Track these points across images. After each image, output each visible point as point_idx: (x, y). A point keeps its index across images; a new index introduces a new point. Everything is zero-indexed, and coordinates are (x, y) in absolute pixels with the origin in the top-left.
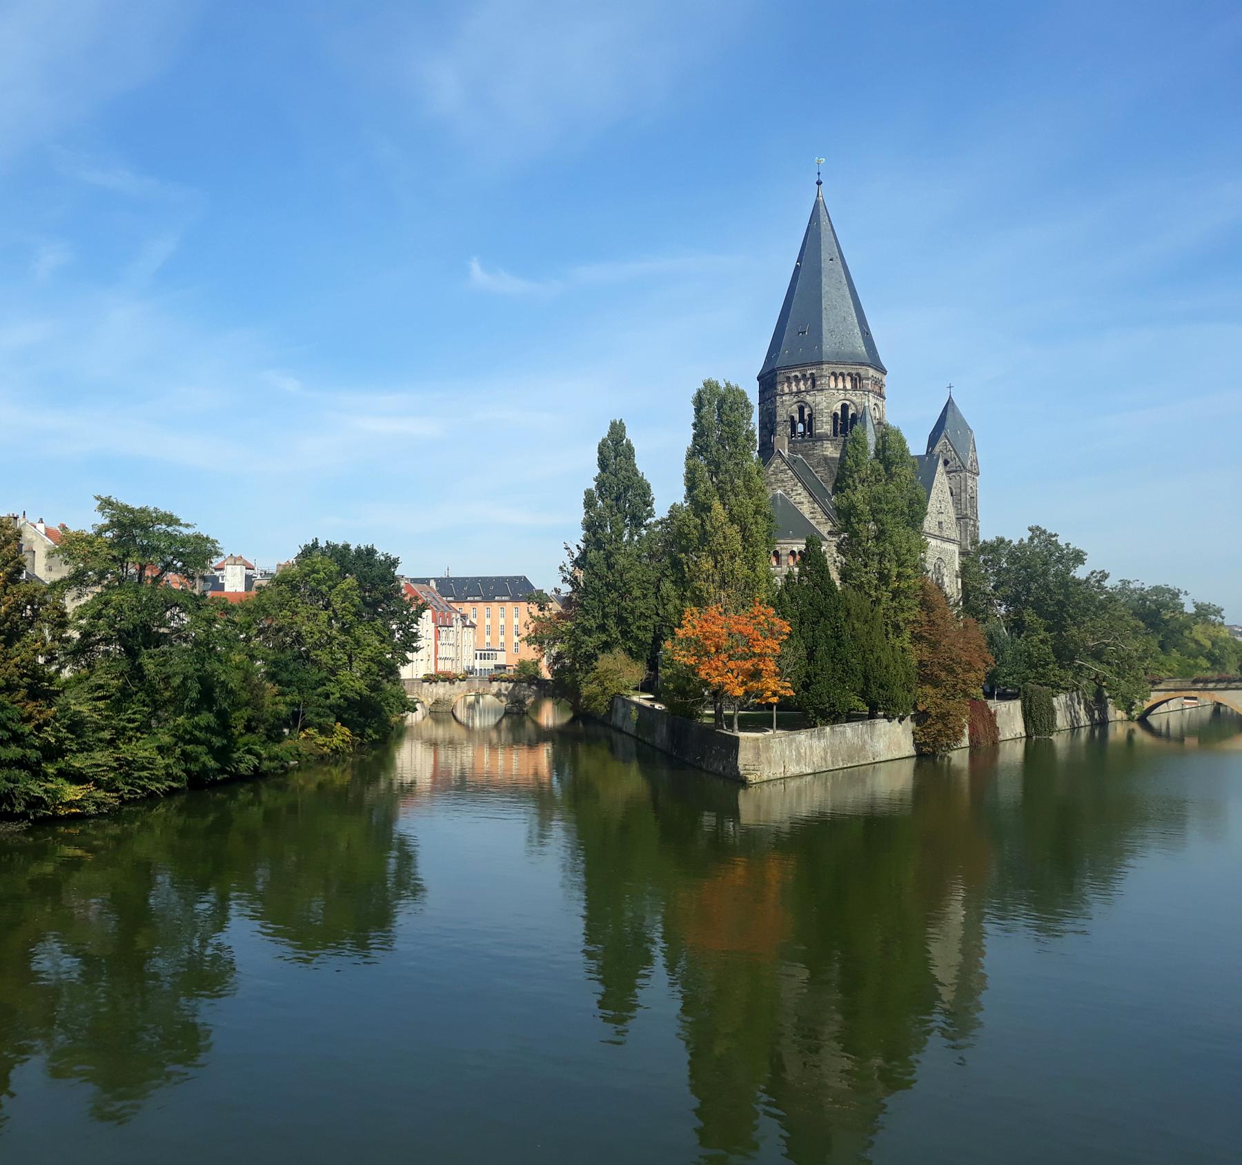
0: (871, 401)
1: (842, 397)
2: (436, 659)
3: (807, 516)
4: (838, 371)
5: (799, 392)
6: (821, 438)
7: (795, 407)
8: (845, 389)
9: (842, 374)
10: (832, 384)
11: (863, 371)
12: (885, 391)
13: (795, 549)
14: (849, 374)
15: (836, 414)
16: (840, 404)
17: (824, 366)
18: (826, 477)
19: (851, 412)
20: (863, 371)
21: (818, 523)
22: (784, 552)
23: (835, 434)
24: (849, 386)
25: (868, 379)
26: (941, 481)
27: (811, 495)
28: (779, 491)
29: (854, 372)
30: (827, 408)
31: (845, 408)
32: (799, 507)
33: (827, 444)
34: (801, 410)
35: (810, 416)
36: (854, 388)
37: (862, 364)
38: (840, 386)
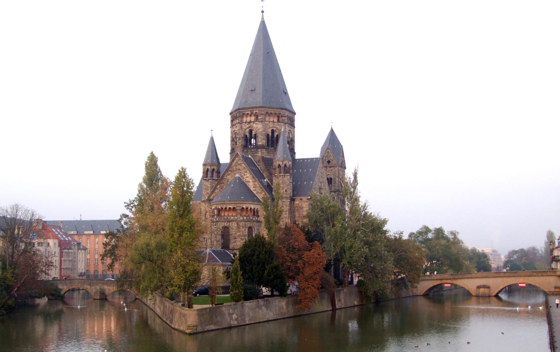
0: (288, 128)
1: (271, 126)
2: (61, 269)
3: (252, 189)
4: (270, 112)
5: (250, 122)
6: (262, 147)
7: (248, 130)
8: (273, 122)
9: (271, 113)
10: (267, 119)
11: (282, 112)
12: (296, 123)
13: (244, 207)
14: (275, 114)
15: (268, 135)
16: (270, 130)
18: (263, 169)
19: (276, 134)
20: (282, 112)
21: (257, 193)
22: (238, 208)
23: (268, 145)
24: (276, 120)
25: (285, 117)
27: (253, 178)
28: (237, 175)
29: (278, 113)
30: (263, 131)
31: (273, 131)
32: (248, 184)
33: (264, 151)
34: (251, 131)
35: (255, 135)
36: (278, 121)
37: (282, 109)
38: (271, 119)
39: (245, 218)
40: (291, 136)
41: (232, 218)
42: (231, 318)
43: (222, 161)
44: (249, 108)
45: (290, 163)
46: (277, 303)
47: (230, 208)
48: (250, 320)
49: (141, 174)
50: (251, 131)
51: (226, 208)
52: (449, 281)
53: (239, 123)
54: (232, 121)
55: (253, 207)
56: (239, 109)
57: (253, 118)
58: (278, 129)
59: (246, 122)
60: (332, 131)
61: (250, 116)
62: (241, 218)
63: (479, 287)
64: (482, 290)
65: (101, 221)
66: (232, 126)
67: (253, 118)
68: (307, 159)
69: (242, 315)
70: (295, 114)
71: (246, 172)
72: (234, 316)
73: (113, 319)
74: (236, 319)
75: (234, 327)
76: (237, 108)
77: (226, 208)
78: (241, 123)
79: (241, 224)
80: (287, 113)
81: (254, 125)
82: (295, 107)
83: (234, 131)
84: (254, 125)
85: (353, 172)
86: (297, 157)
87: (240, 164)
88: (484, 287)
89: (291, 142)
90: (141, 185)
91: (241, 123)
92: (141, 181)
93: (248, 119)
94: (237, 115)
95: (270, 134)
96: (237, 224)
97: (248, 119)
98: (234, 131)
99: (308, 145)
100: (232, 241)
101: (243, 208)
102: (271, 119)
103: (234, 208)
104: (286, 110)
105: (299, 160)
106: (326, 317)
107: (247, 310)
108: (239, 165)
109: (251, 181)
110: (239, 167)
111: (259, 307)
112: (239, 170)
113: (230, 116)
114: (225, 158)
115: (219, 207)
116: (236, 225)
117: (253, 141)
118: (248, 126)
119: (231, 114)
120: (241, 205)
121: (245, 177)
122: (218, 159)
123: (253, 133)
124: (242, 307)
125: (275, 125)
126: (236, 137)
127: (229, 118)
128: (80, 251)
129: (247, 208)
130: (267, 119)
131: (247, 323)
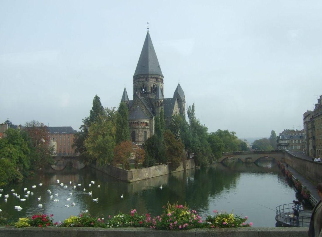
1: (153, 83)
5: (143, 81)
7: (142, 85)
9: (153, 77)
13: (142, 122)
14: (155, 77)
15: (152, 87)
16: (152, 85)
17: (149, 75)
19: (155, 87)
23: (152, 92)
24: (155, 80)
26: (176, 104)
29: (156, 77)
31: (154, 86)
33: (150, 95)
34: (143, 86)
35: (146, 87)
36: (157, 81)
39: (142, 127)
40: (162, 88)
41: (136, 127)
42: (146, 175)
43: (130, 100)
44: (143, 75)
45: (163, 101)
46: (163, 167)
47: (135, 122)
48: (153, 176)
49: (90, 106)
50: (143, 86)
51: (133, 122)
52: (233, 156)
53: (138, 82)
54: (134, 81)
55: (146, 121)
56: (138, 75)
57: (144, 80)
58: (156, 84)
59: (141, 82)
60: (179, 85)
61: (143, 78)
62: (141, 127)
63: (247, 159)
64: (248, 160)
65: (63, 127)
66: (134, 83)
67: (144, 80)
68: (170, 99)
69: (149, 173)
70: (163, 77)
71: (142, 105)
72: (147, 174)
73: (188, 182)
74: (148, 175)
75: (147, 179)
76: (136, 74)
77: (133, 122)
78: (139, 82)
79: (140, 130)
80: (160, 77)
81: (145, 83)
82: (164, 73)
83: (135, 85)
84: (145, 83)
85: (192, 105)
86: (165, 97)
87: (139, 101)
88: (249, 158)
89: (162, 90)
90: (91, 111)
91: (139, 82)
92: (91, 109)
93: (142, 80)
94: (136, 78)
95: (153, 87)
96: (139, 130)
97: (142, 80)
98: (135, 85)
99: (168, 93)
100: (136, 138)
101: (141, 122)
102: (153, 80)
103: (137, 122)
104: (159, 75)
105: (166, 99)
106: (182, 173)
107: (151, 171)
108: (139, 101)
109: (144, 109)
110: (139, 103)
111: (156, 169)
112: (139, 104)
113: (133, 78)
114: (131, 98)
115: (130, 122)
116: (138, 130)
117: (143, 90)
118: (142, 83)
119: (134, 77)
120: (141, 121)
121: (142, 107)
122: (128, 99)
123: (145, 86)
124: (150, 169)
125: (155, 83)
126: (136, 88)
127: (132, 79)
128: (54, 142)
129: (143, 122)
130: (151, 80)
131: (152, 177)
